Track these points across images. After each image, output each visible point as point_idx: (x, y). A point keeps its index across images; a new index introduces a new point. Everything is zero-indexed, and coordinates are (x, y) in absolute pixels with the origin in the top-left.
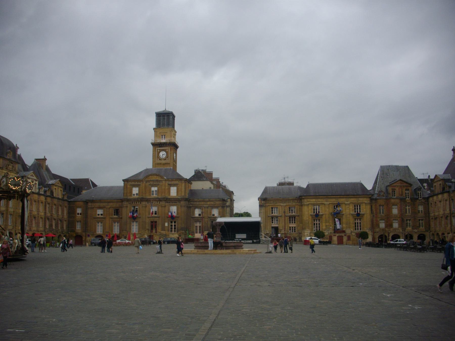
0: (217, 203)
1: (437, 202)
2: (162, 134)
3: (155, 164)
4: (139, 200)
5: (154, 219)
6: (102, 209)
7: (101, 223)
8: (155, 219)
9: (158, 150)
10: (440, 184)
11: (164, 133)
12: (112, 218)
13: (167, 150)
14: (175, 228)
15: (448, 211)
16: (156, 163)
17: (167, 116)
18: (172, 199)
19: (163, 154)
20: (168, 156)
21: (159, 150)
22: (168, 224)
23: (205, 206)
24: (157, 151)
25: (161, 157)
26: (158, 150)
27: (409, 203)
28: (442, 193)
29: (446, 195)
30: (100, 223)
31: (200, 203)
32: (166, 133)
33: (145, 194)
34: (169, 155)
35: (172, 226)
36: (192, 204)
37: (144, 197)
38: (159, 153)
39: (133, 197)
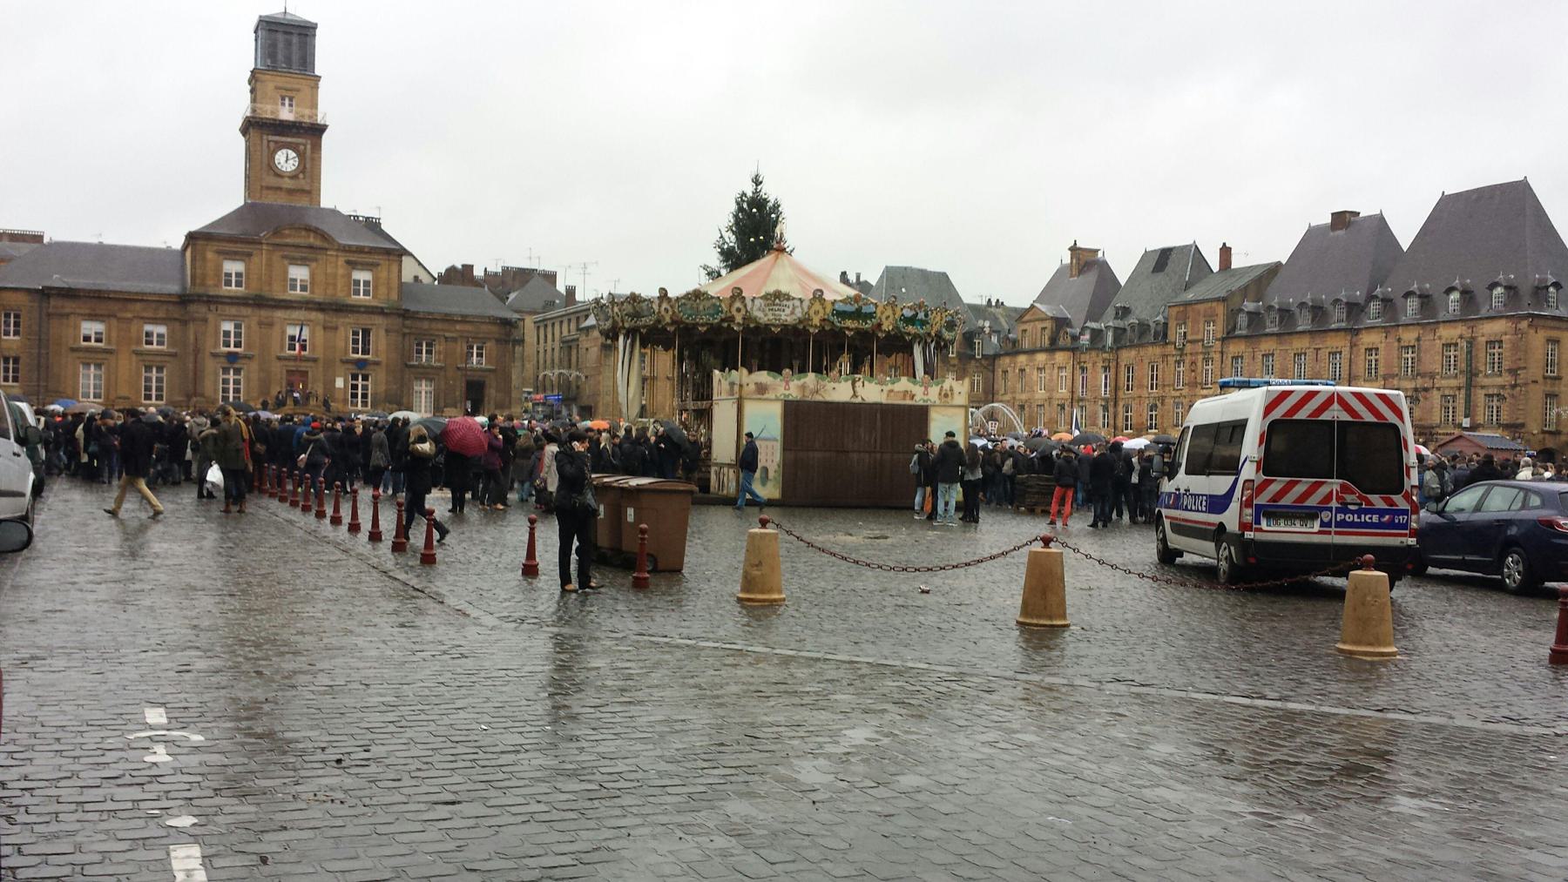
0: (484, 328)
1: (1028, 370)
2: (284, 93)
3: (262, 187)
4: (251, 302)
5: (298, 363)
6: (102, 321)
7: (98, 366)
8: (303, 366)
9: (269, 141)
10: (1044, 329)
11: (291, 90)
12: (137, 353)
13: (302, 147)
14: (364, 396)
15: (1064, 392)
16: (264, 184)
17: (300, 34)
18: (360, 306)
19: (286, 160)
20: (305, 167)
21: (272, 145)
22: (346, 382)
23: (447, 334)
24: (268, 147)
25: (279, 167)
26: (269, 141)
27: (954, 366)
28: (1053, 348)
29: (1060, 357)
30: (92, 367)
31: (434, 325)
32: (298, 90)
33: (270, 284)
34: (308, 166)
35: (355, 387)
36: (407, 327)
37: (266, 294)
38: (275, 152)
39: (225, 290)
